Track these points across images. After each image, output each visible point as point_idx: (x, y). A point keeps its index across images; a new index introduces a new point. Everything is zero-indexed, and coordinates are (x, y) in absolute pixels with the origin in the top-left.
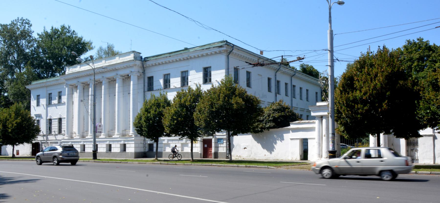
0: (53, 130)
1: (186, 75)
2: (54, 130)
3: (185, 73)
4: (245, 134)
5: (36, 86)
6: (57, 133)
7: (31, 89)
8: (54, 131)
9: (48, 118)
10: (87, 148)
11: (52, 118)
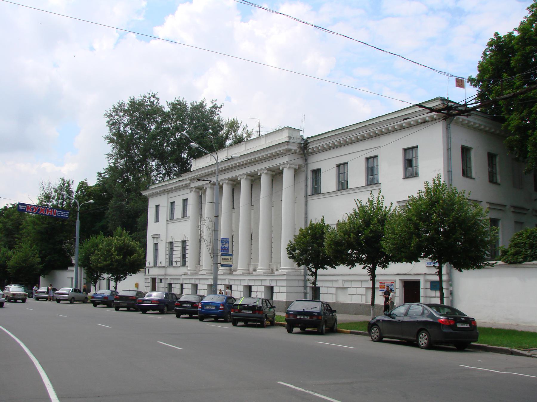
0: (174, 260)
1: (414, 156)
2: (176, 261)
3: (411, 152)
4: (472, 268)
5: (153, 191)
6: (179, 264)
7: (149, 196)
8: (176, 262)
9: (169, 240)
10: (199, 289)
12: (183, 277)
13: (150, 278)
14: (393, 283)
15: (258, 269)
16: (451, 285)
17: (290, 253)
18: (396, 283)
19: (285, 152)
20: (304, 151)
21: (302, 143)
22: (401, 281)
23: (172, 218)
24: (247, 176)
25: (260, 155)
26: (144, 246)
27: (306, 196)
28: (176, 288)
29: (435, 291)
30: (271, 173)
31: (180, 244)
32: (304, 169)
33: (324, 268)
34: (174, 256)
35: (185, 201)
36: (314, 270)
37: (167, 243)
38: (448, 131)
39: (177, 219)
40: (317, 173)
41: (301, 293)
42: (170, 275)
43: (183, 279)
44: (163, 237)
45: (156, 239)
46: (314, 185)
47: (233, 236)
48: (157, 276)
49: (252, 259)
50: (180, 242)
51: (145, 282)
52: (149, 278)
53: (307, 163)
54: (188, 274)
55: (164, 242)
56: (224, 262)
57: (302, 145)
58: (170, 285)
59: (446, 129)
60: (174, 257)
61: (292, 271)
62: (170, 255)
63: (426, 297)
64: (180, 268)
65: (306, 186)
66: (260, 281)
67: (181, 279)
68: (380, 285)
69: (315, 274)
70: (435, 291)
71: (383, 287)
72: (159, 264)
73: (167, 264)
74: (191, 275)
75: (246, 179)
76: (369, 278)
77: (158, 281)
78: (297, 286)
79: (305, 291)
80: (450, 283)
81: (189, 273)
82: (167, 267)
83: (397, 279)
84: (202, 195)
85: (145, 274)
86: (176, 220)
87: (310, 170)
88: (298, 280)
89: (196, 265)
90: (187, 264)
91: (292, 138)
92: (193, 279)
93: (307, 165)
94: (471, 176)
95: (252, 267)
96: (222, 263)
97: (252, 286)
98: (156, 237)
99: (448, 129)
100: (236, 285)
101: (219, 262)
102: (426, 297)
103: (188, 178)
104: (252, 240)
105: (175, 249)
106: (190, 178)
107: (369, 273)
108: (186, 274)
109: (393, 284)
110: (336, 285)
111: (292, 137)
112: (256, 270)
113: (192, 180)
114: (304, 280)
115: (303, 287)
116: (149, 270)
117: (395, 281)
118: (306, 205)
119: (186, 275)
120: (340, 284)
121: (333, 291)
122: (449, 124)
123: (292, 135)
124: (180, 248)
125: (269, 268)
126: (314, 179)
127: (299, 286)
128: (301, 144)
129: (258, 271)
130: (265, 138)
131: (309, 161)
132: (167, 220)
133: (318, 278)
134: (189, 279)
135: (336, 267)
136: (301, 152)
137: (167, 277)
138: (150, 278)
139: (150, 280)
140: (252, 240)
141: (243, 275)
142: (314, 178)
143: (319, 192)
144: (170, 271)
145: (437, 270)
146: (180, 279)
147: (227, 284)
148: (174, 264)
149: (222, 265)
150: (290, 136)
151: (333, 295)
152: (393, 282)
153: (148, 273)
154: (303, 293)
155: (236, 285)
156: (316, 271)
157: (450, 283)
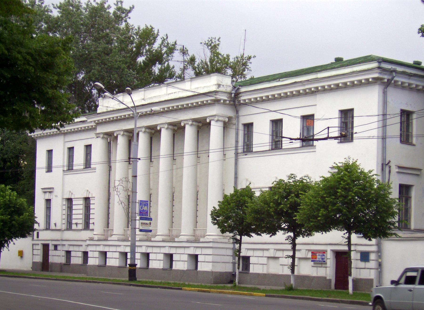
0: (74, 221)
2: (76, 222)
6: (80, 227)
8: (77, 224)
11: (72, 197)
12: (88, 242)
13: (40, 244)
14: (325, 253)
15: (181, 235)
16: (380, 257)
17: (214, 219)
18: (327, 253)
19: (212, 102)
20: (234, 102)
21: (233, 93)
22: (333, 251)
23: (70, 167)
24: (168, 125)
25: (185, 103)
26: (32, 201)
27: (237, 154)
28: (76, 257)
29: (365, 263)
30: (197, 124)
31: (82, 202)
32: (234, 121)
33: (250, 236)
34: (74, 217)
35: (88, 147)
36: (238, 237)
37: (64, 200)
38: (385, 95)
39: (77, 170)
40: (249, 126)
41: (229, 263)
42: (72, 240)
43: (88, 245)
44: (58, 191)
45: (48, 194)
46: (246, 141)
47: (150, 195)
48: (50, 241)
49: (173, 223)
50: (82, 199)
51: (33, 249)
52: (38, 244)
53: (239, 115)
54: (94, 239)
56: (143, 227)
57: (233, 95)
58: (68, 253)
59: (383, 93)
60: (73, 218)
61: (219, 238)
62: (68, 215)
63: (357, 268)
65: (237, 142)
66: (175, 249)
67: (84, 246)
68: (312, 255)
69: (239, 242)
70: (365, 263)
71: (314, 257)
72: (52, 227)
73: (64, 227)
74: (99, 240)
75: (167, 129)
76: (290, 247)
77: (51, 248)
78: (225, 255)
79: (234, 261)
80: (379, 254)
81: (96, 238)
82: (64, 230)
83: (329, 249)
84: (112, 142)
85: (33, 239)
86: (77, 171)
87: (242, 124)
88: (227, 248)
89: (105, 229)
90: (91, 226)
91: (221, 86)
92: (102, 246)
93: (238, 117)
94: (412, 142)
95: (174, 233)
96: (141, 228)
97: (174, 254)
98: (49, 190)
99: (385, 93)
100: (154, 253)
101: (137, 227)
102: (357, 268)
103: (95, 121)
104: (173, 200)
105: (74, 207)
106: (96, 122)
107: (290, 242)
108: (91, 239)
109: (324, 254)
110: (267, 254)
111: (221, 85)
112: (178, 236)
113: (99, 123)
114: (233, 249)
115: (232, 256)
116: (38, 234)
117: (327, 251)
118: (236, 164)
119: (92, 240)
120: (271, 253)
121: (264, 261)
122: (386, 88)
123: (222, 82)
124: (81, 207)
125: (194, 235)
126: (246, 134)
127: (227, 256)
128: (232, 94)
129: (180, 237)
130: (190, 82)
131: (241, 113)
132: (63, 171)
133: (243, 246)
134: (96, 245)
135: (262, 234)
136: (232, 103)
137: (64, 243)
138: (40, 244)
139: (40, 247)
140: (173, 200)
141: (163, 241)
142: (246, 132)
143: (251, 150)
144: (68, 235)
145: (347, 240)
146: (82, 245)
147: (144, 251)
148: (74, 227)
149: (141, 231)
150: (219, 83)
151: (264, 265)
152: (324, 252)
153: (38, 237)
154: (232, 263)
155: (154, 253)
156: (241, 238)
157: (379, 254)
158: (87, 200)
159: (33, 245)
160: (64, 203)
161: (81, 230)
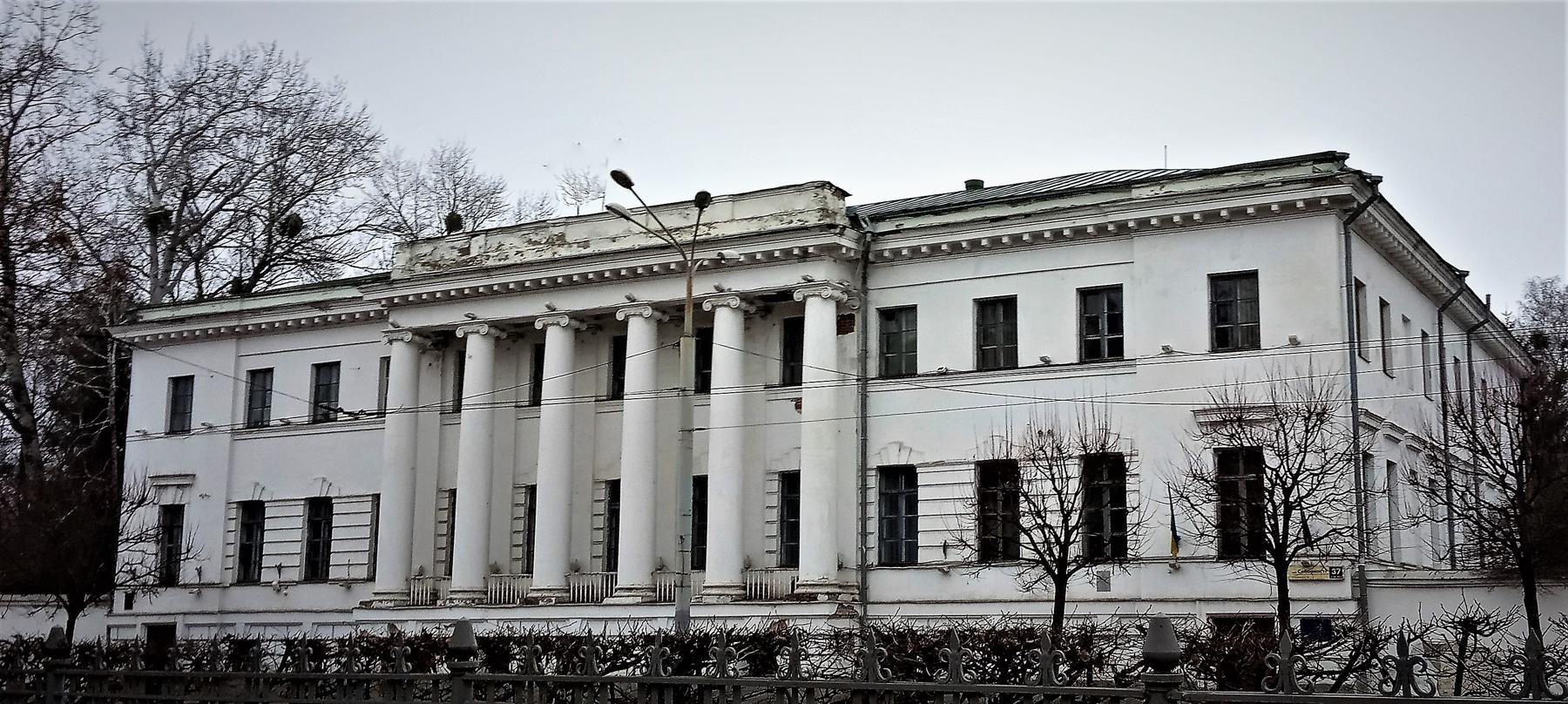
6: (295, 575)
8: (280, 568)
50: (303, 503)
52: (135, 626)
55: (219, 497)
64: (300, 586)
73: (230, 577)
82: (231, 585)
153: (129, 605)
158: (320, 511)
159: (109, 629)
160: (233, 514)
161: (297, 582)
